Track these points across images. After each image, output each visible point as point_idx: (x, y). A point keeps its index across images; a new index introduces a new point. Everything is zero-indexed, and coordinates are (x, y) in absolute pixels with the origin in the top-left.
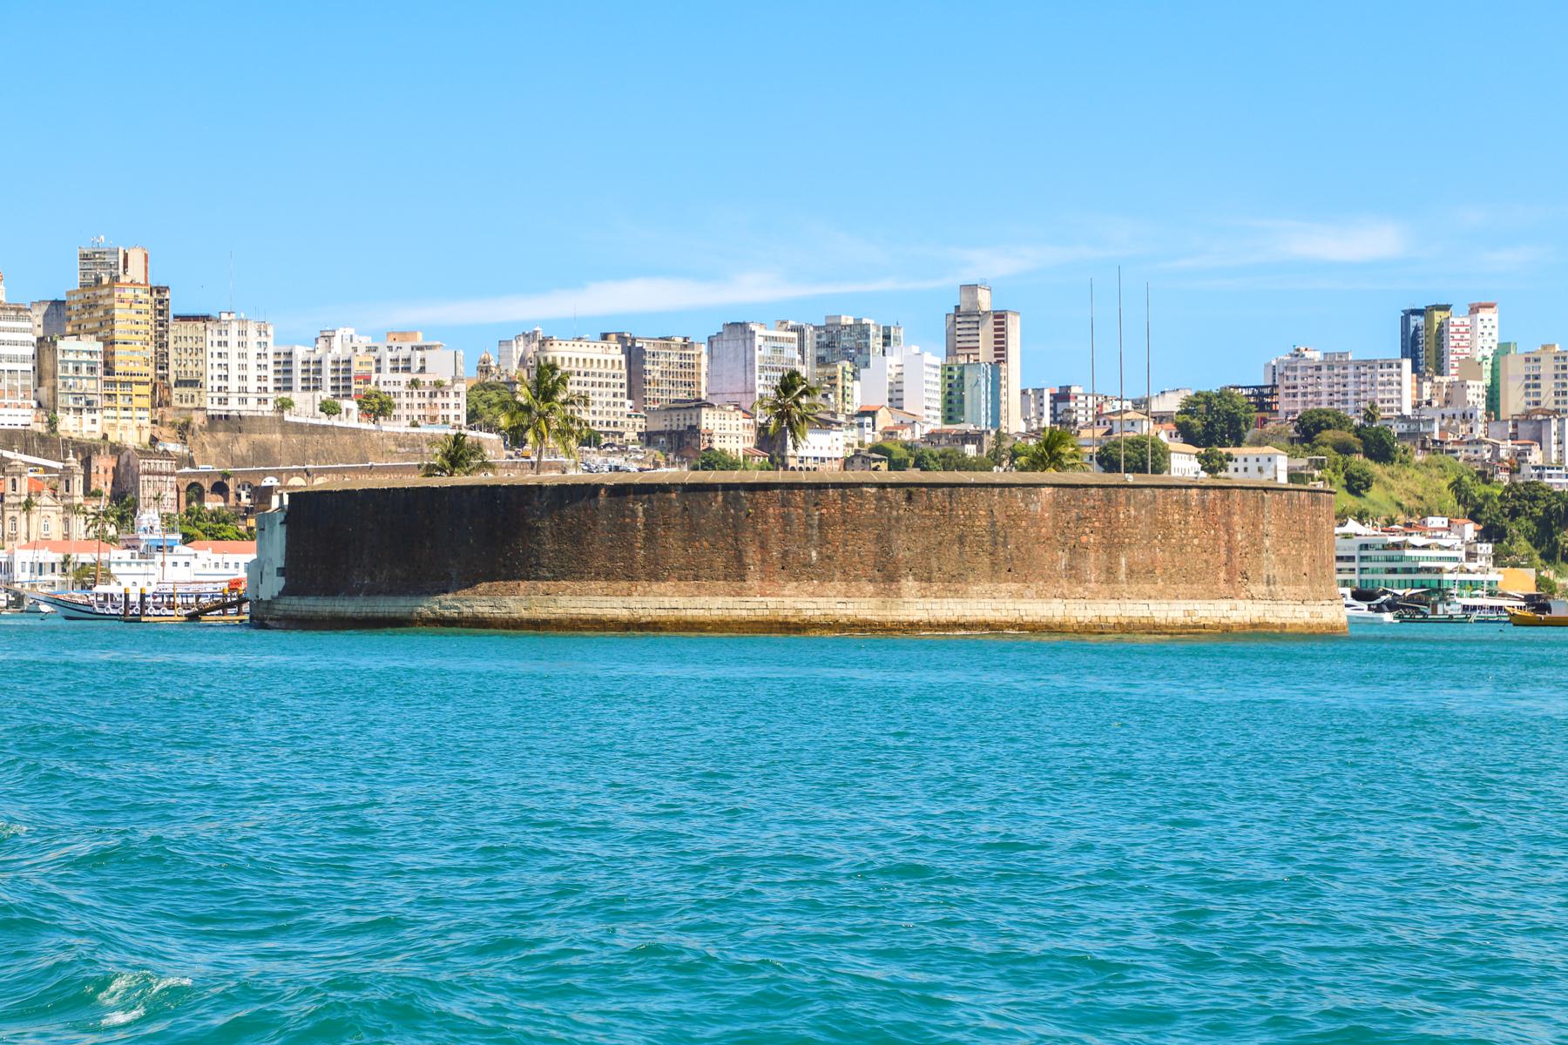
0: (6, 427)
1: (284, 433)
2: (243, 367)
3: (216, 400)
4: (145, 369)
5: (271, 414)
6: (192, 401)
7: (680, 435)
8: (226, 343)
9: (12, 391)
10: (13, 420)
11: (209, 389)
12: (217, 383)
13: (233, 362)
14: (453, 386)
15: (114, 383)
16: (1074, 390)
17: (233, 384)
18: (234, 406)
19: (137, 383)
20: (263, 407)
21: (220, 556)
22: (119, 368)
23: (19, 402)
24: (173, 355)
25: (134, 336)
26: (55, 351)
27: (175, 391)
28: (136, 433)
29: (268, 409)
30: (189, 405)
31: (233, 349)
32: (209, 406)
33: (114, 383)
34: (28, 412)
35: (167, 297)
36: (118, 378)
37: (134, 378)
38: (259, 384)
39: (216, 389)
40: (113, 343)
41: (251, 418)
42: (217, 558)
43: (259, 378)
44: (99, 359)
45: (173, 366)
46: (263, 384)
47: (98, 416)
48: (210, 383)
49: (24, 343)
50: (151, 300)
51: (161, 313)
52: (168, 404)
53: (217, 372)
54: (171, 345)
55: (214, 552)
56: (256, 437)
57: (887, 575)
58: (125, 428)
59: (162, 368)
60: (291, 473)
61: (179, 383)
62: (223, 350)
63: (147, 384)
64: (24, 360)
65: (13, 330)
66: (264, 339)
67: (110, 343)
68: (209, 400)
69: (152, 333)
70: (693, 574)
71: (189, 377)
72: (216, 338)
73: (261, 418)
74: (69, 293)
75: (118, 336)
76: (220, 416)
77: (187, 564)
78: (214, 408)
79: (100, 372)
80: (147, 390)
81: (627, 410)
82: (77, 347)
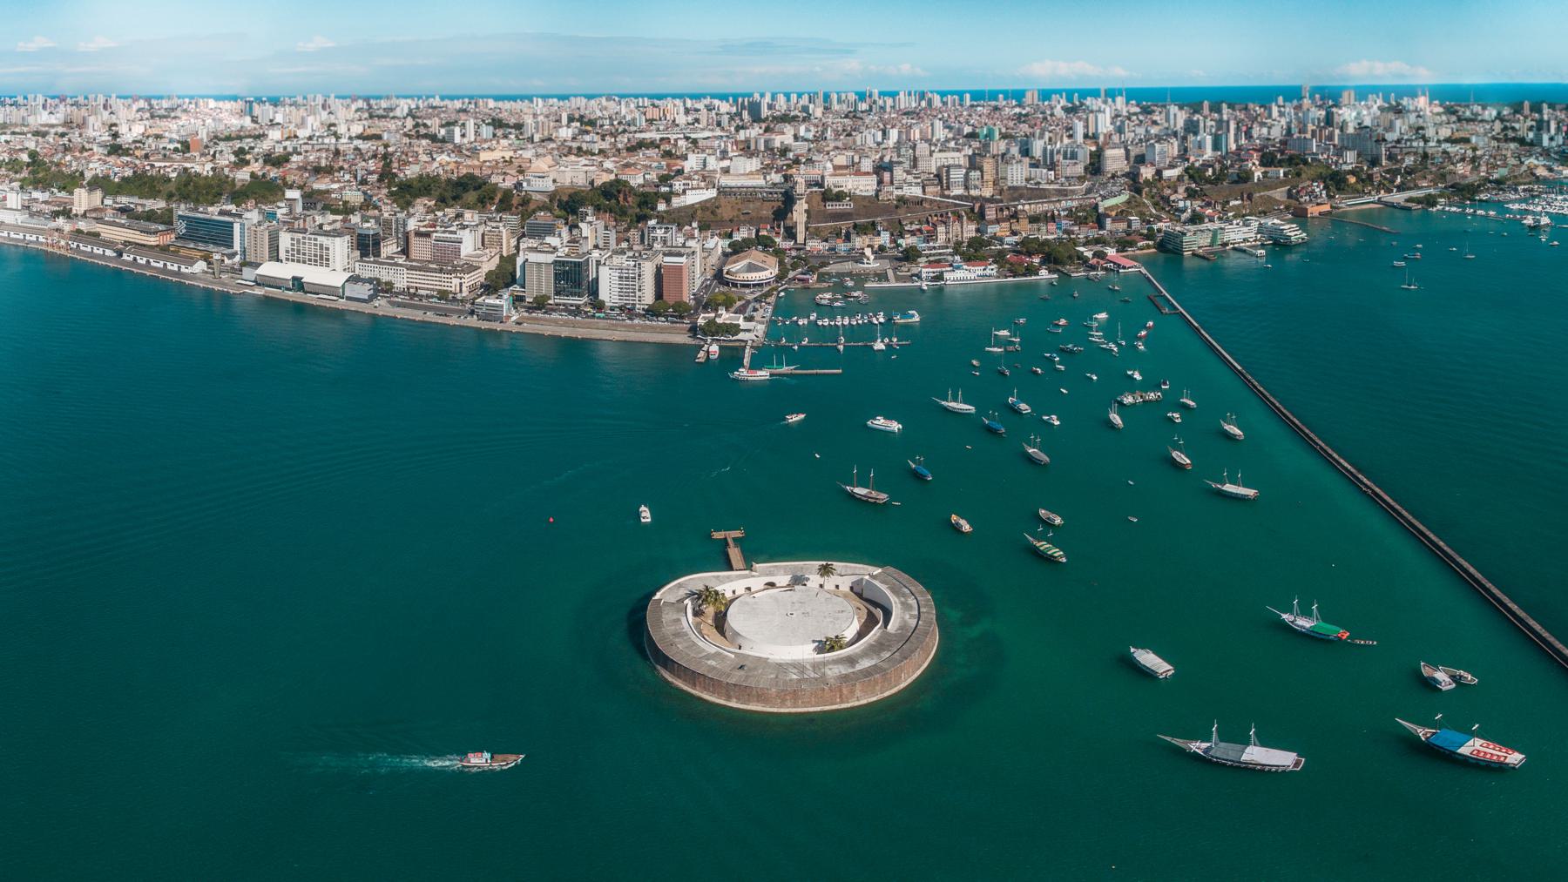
9: (959, 186)
13: (1015, 174)
17: (1015, 179)
18: (1015, 184)
31: (1015, 170)
78: (1009, 184)
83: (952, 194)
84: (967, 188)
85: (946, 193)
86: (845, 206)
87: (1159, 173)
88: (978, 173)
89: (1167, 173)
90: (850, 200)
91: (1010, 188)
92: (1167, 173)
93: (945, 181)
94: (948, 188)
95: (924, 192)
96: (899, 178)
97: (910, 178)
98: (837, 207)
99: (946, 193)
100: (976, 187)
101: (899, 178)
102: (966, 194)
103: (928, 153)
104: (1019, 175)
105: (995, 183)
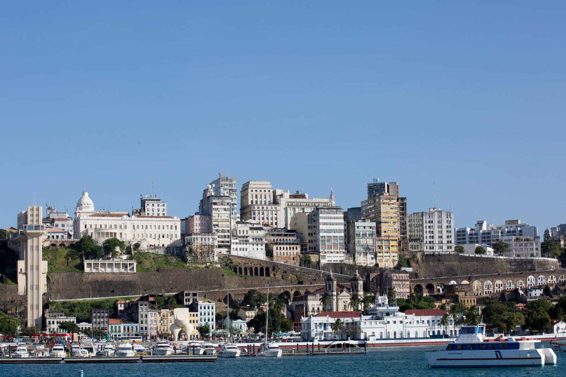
0: (333, 262)
1: (460, 261)
2: (441, 232)
3: (428, 248)
4: (395, 234)
5: (453, 253)
6: (418, 248)
8: (432, 222)
9: (335, 245)
10: (336, 259)
11: (425, 242)
12: (429, 240)
13: (436, 230)
14: (534, 240)
17: (436, 240)
18: (437, 249)
19: (392, 240)
20: (450, 250)
21: (419, 317)
22: (383, 234)
23: (338, 251)
24: (408, 228)
25: (390, 219)
26: (354, 227)
27: (410, 244)
28: (392, 263)
29: (452, 251)
30: (416, 250)
31: (436, 224)
32: (425, 250)
34: (342, 255)
35: (405, 202)
36: (383, 238)
37: (390, 238)
38: (448, 239)
39: (428, 242)
40: (380, 223)
43: (448, 237)
45: (408, 234)
46: (450, 240)
48: (425, 240)
49: (340, 224)
50: (398, 203)
51: (403, 209)
52: (407, 250)
53: (429, 235)
54: (408, 224)
55: (416, 315)
56: (445, 263)
58: (386, 261)
59: (403, 234)
60: (463, 279)
61: (411, 240)
62: (432, 225)
63: (397, 240)
64: (340, 231)
65: (335, 218)
66: (449, 219)
67: (379, 223)
68: (425, 248)
69: (399, 218)
71: (416, 238)
72: (428, 220)
73: (449, 255)
74: (362, 203)
75: (382, 220)
76: (430, 255)
77: (401, 322)
78: (427, 251)
80: (395, 243)
83: (323, 262)
84: (350, 250)
88: (368, 223)
90: (131, 258)
94: (316, 250)
95: (269, 253)
96: (223, 226)
97: (242, 228)
98: (109, 270)
100: (367, 250)
101: (223, 226)
102: (351, 262)
103: (270, 199)
104: (445, 235)
105: (403, 242)
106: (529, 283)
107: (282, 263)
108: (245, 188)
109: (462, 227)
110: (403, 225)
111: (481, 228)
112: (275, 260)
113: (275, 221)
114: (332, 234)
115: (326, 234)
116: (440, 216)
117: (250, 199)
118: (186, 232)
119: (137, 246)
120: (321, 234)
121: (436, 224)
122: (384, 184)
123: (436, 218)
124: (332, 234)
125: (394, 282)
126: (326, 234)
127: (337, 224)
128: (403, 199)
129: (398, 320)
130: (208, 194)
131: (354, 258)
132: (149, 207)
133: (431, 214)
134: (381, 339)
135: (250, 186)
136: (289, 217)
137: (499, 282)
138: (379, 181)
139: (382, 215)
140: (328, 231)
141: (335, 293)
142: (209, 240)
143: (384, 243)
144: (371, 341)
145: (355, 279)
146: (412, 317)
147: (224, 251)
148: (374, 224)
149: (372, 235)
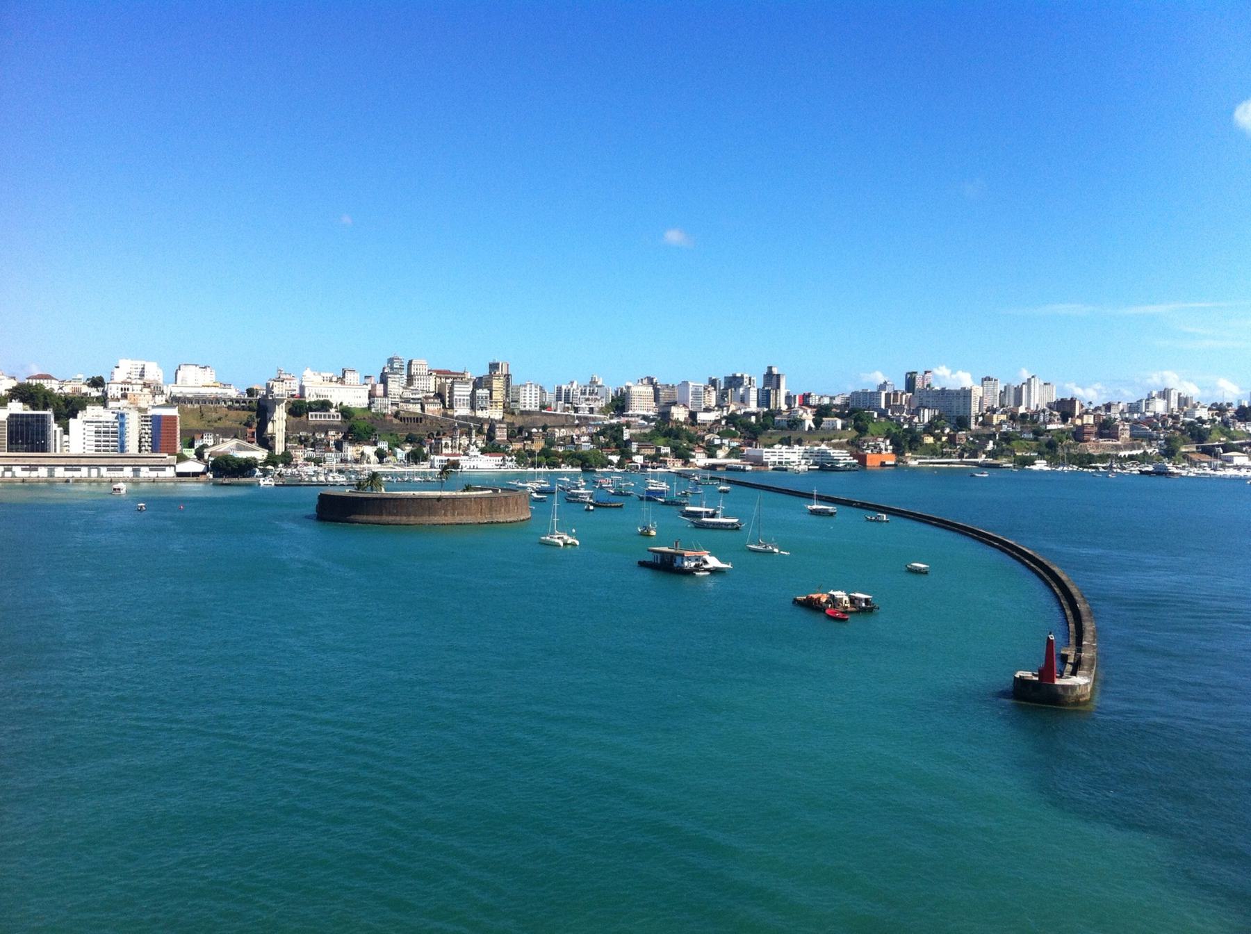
7: (665, 413)
12: (523, 401)
13: (528, 395)
15: (492, 402)
16: (812, 394)
17: (528, 402)
18: (528, 408)
22: (494, 398)
27: (512, 404)
31: (528, 392)
33: (492, 402)
41: (533, 411)
42: (492, 458)
44: (489, 395)
47: (487, 411)
57: (408, 515)
61: (512, 402)
64: (467, 396)
70: (374, 514)
73: (535, 411)
75: (494, 389)
78: (522, 408)
79: (488, 399)
80: (502, 404)
81: (654, 405)
82: (480, 392)
83: (456, 414)
84: (473, 408)
85: (449, 412)
86: (334, 415)
87: (693, 415)
88: (486, 391)
89: (702, 417)
91: (523, 413)
92: (702, 417)
93: (447, 399)
94: (451, 407)
95: (423, 409)
99: (449, 412)
106: (582, 431)
107: (431, 414)
108: (410, 363)
109: (559, 385)
110: (507, 391)
111: (572, 386)
112: (426, 413)
113: (428, 386)
114: (462, 398)
115: (458, 398)
116: (531, 387)
117: (413, 371)
118: (372, 395)
119: (341, 404)
120: (455, 397)
121: (528, 392)
122: (498, 364)
123: (528, 389)
124: (462, 398)
125: (497, 429)
126: (458, 398)
127: (464, 391)
128: (508, 375)
129: (479, 459)
130: (386, 371)
131: (475, 412)
132: (348, 375)
133: (525, 386)
134: (470, 468)
135: (413, 363)
136: (438, 383)
137: (563, 430)
138: (496, 362)
139: (494, 386)
140: (460, 395)
141: (458, 437)
142: (386, 401)
143: (494, 404)
144: (464, 469)
145: (470, 429)
146: (488, 458)
147: (395, 408)
148: (489, 392)
149: (486, 398)
